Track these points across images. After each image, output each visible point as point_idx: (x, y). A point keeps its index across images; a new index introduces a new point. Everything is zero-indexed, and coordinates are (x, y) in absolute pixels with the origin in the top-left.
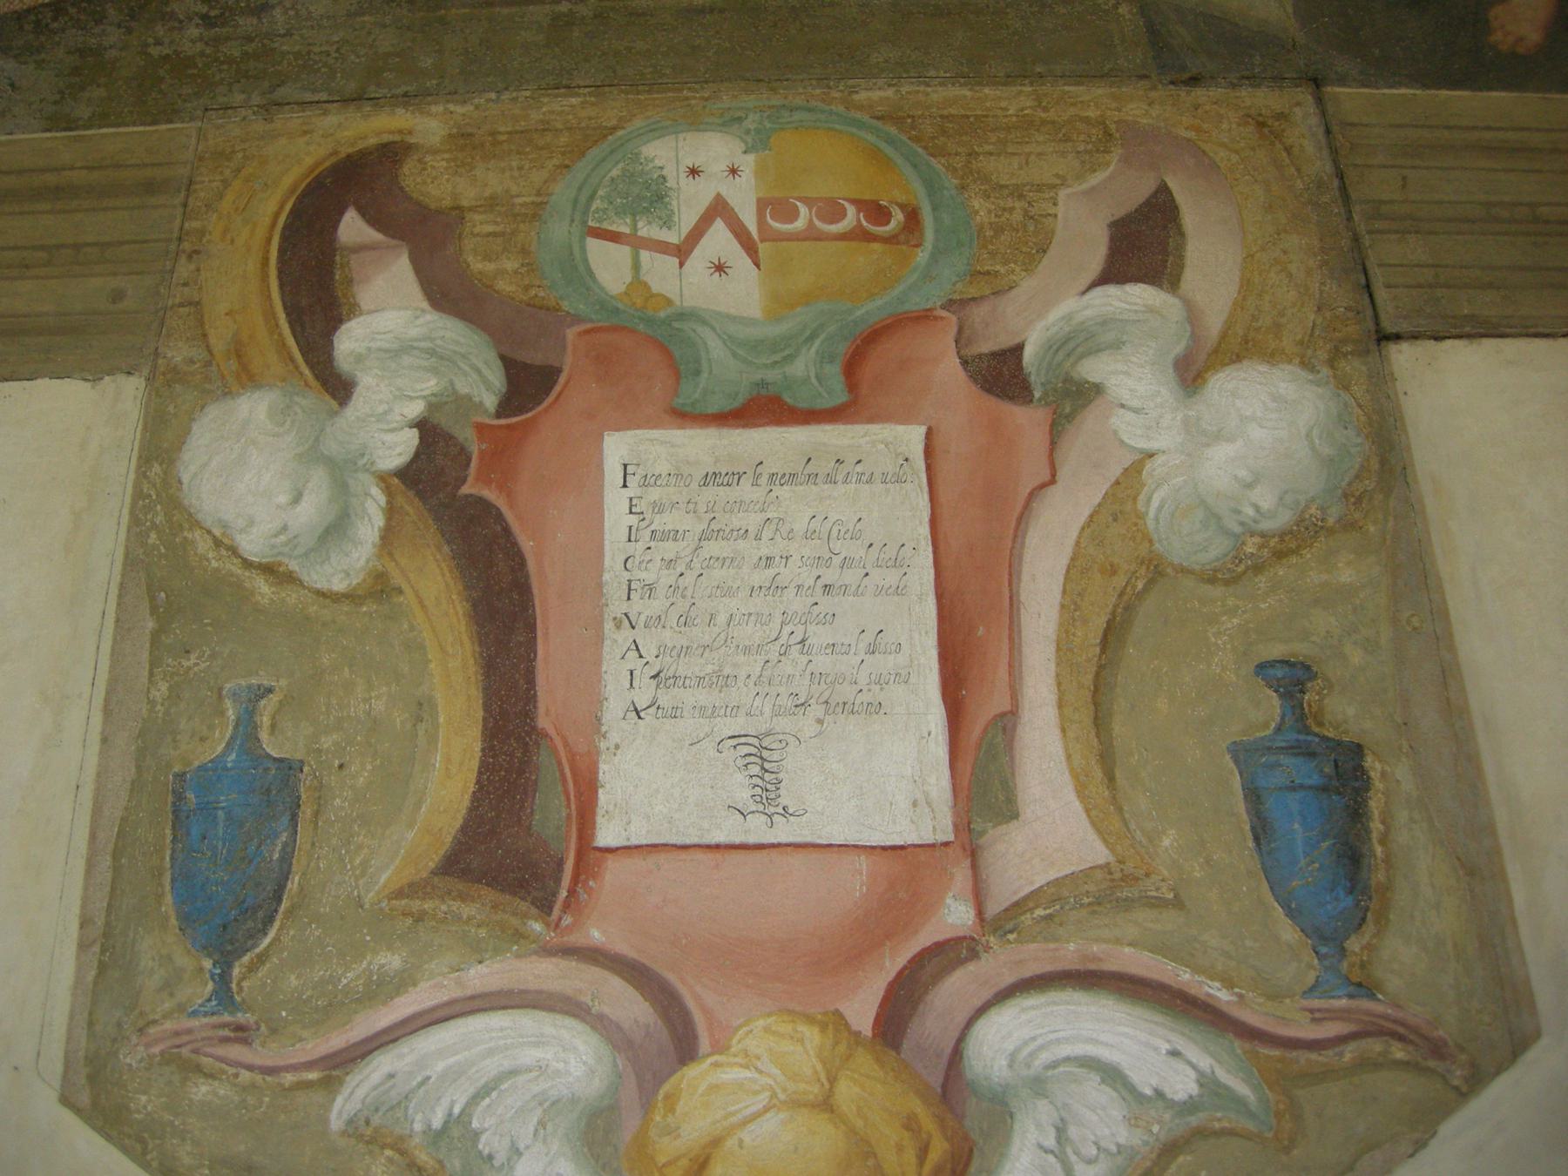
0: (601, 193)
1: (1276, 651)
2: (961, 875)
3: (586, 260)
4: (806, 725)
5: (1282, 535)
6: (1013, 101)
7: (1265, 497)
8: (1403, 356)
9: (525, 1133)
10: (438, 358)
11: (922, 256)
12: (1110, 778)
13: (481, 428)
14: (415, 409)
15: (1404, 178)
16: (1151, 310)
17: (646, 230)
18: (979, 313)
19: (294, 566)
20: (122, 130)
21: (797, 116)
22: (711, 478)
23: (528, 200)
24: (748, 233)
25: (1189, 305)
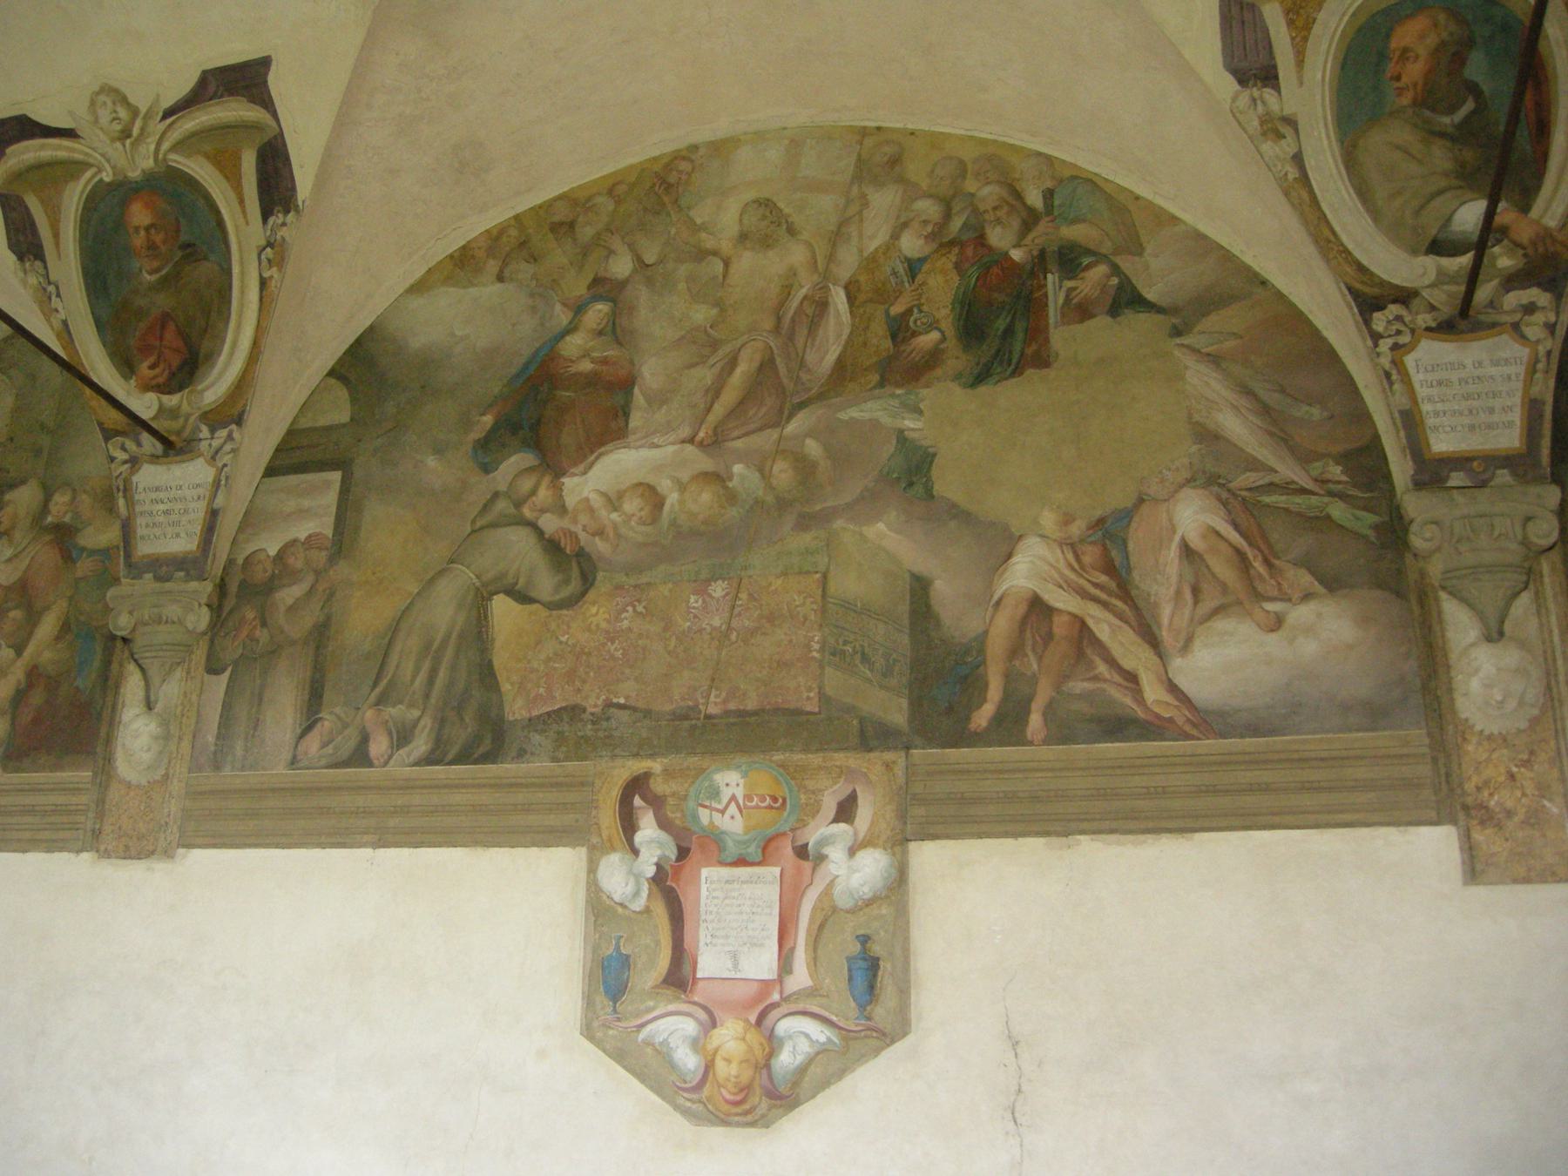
6: (815, 759)
10: (661, 845)
11: (786, 814)
13: (672, 866)
17: (715, 805)
18: (798, 832)
19: (627, 904)
21: (757, 765)
22: (727, 882)
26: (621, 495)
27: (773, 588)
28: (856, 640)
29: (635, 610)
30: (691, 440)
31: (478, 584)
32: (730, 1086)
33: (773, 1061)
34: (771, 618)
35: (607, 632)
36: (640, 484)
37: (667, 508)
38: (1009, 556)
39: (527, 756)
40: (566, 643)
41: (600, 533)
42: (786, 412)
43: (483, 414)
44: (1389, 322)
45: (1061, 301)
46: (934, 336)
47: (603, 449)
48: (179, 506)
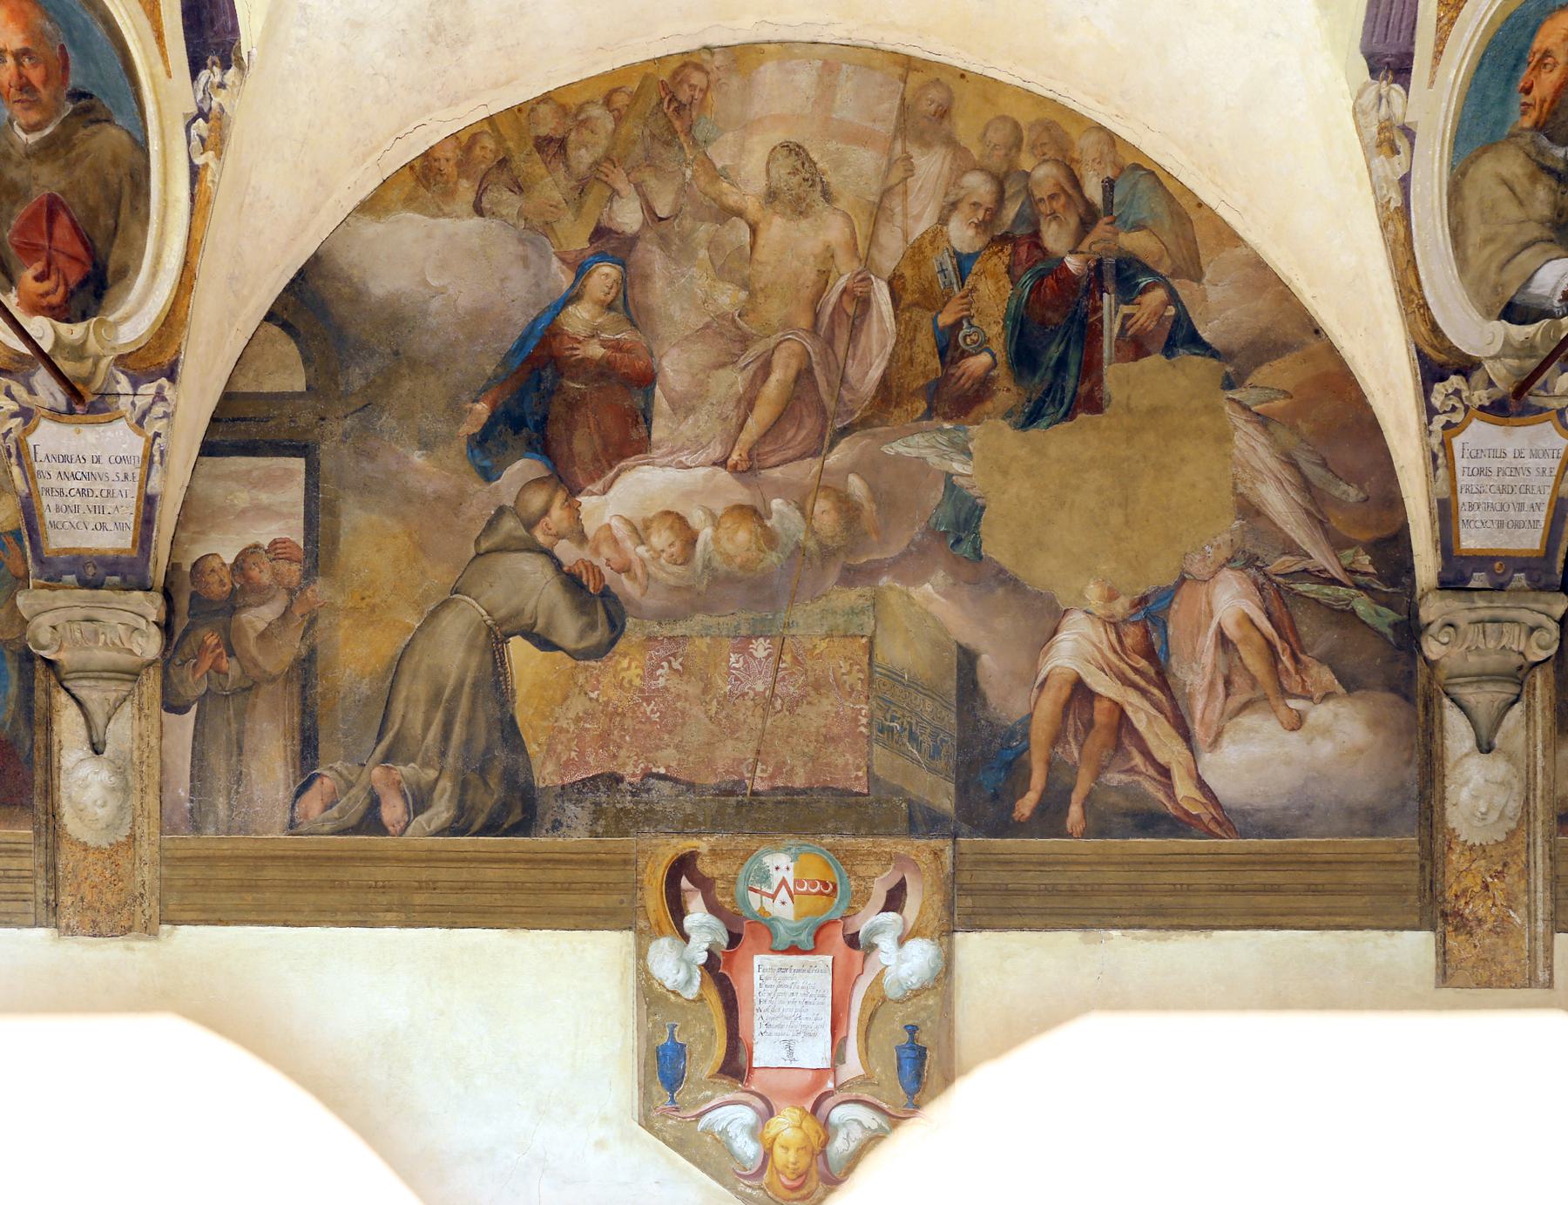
1: (910, 1022)
4: (799, 1038)
5: (917, 990)
6: (865, 843)
7: (914, 979)
8: (958, 936)
9: (738, 1132)
11: (836, 901)
14: (706, 946)
17: (764, 889)
18: (849, 921)
25: (904, 919)
26: (647, 524)
27: (817, 651)
28: (904, 716)
29: (670, 667)
30: (722, 463)
31: (489, 622)
32: (788, 1172)
33: (828, 1148)
34: (817, 686)
35: (642, 691)
36: (668, 513)
37: (699, 546)
38: (1055, 632)
39: (564, 829)
40: (597, 700)
41: (626, 569)
42: (827, 443)
43: (476, 401)
44: (1447, 395)
45: (1116, 330)
46: (985, 358)
47: (623, 464)
48: (98, 486)
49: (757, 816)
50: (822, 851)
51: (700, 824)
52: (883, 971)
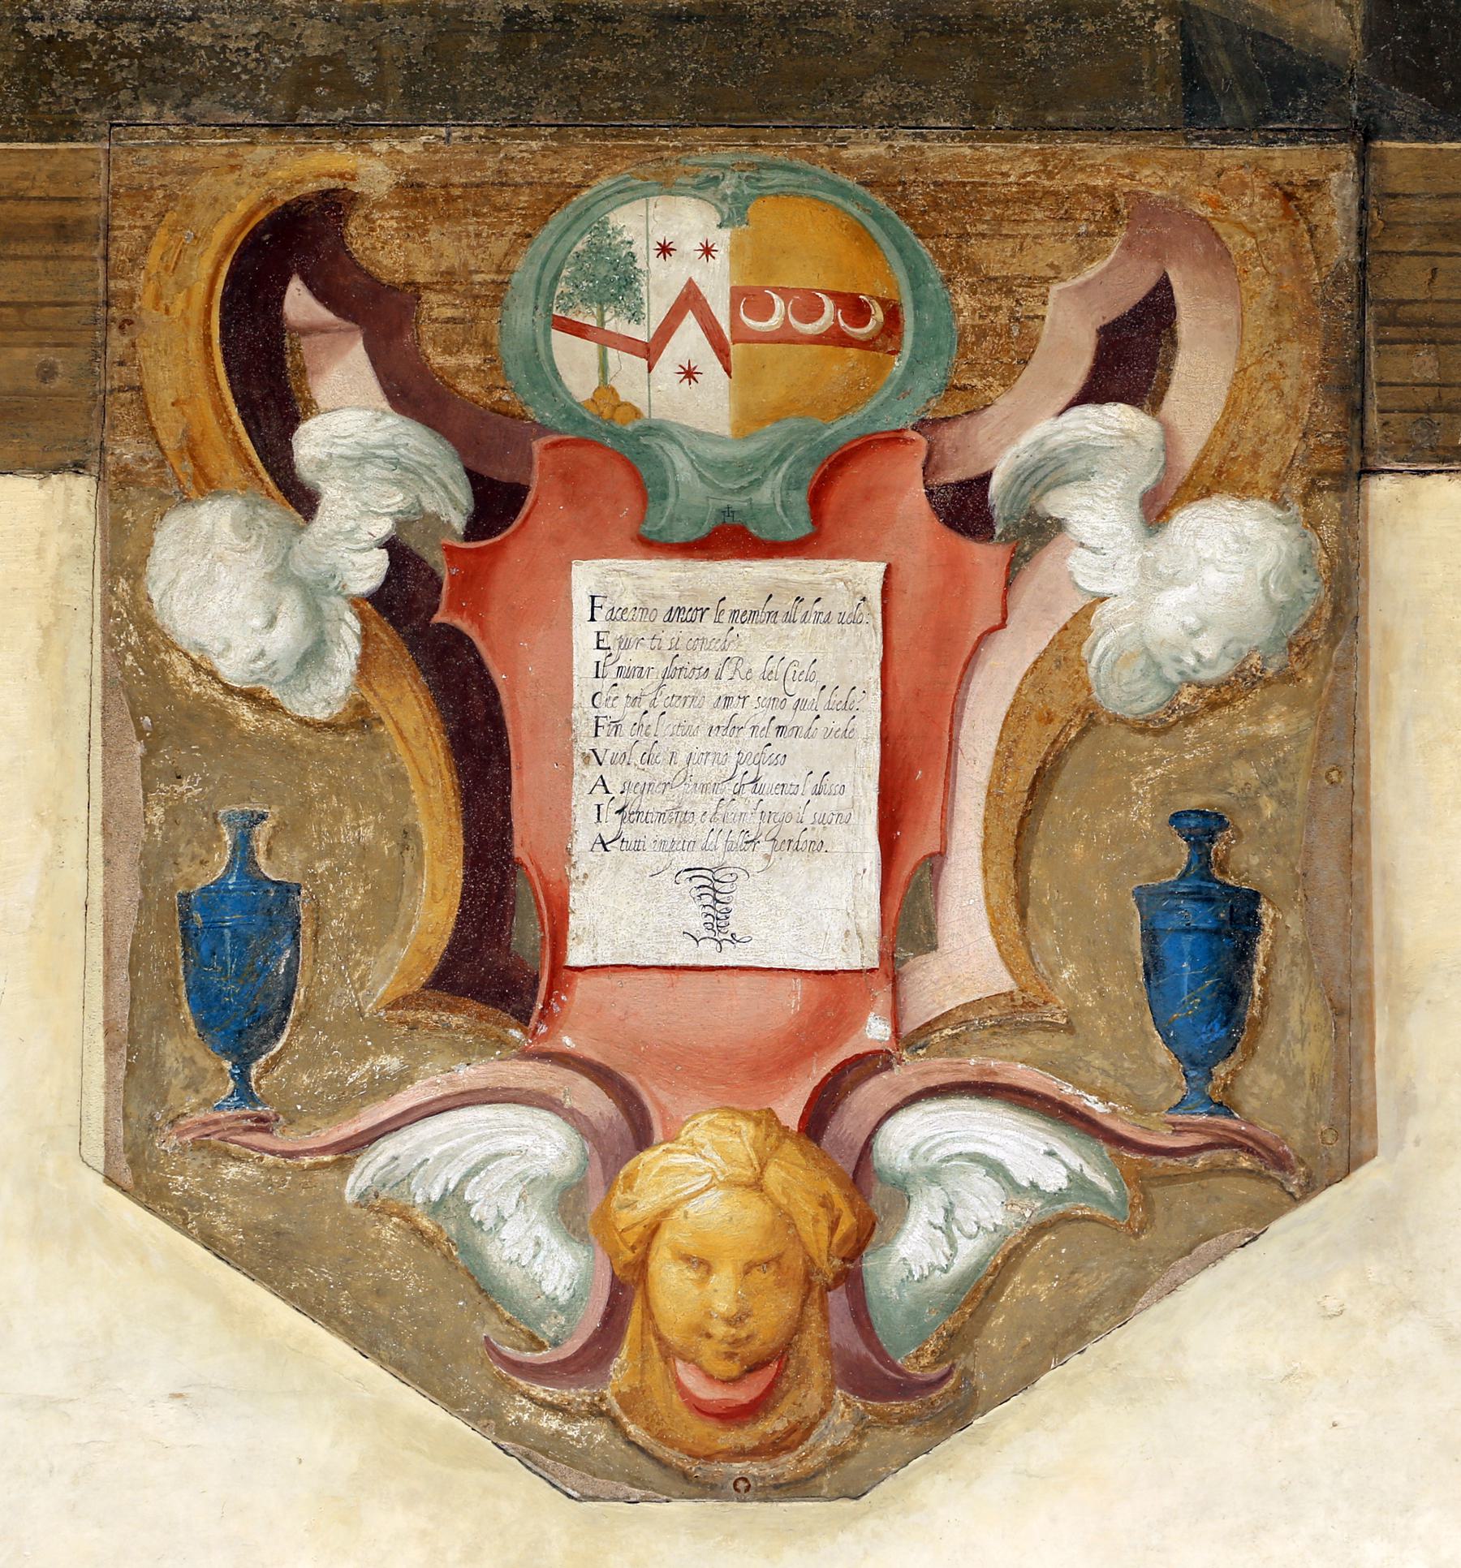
0: (565, 273)
1: (1194, 801)
2: (883, 998)
3: (551, 359)
4: (754, 860)
7: (1208, 646)
8: (1382, 490)
10: (403, 470)
11: (898, 365)
12: (1023, 915)
13: (450, 550)
14: (383, 528)
15: (1434, 271)
16: (1127, 435)
17: (616, 324)
18: (950, 435)
19: (274, 693)
20: (14, 146)
22: (675, 614)
23: (488, 277)
24: (720, 331)
25: (1167, 431)
49: (585, 65)
50: (841, 190)
51: (362, 93)
52: (1084, 615)
